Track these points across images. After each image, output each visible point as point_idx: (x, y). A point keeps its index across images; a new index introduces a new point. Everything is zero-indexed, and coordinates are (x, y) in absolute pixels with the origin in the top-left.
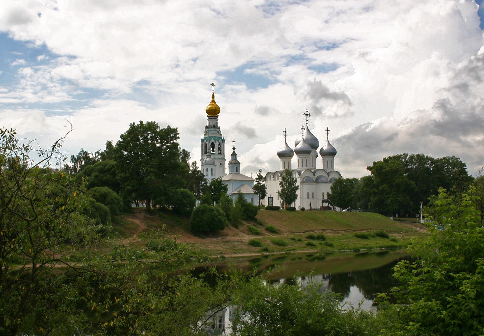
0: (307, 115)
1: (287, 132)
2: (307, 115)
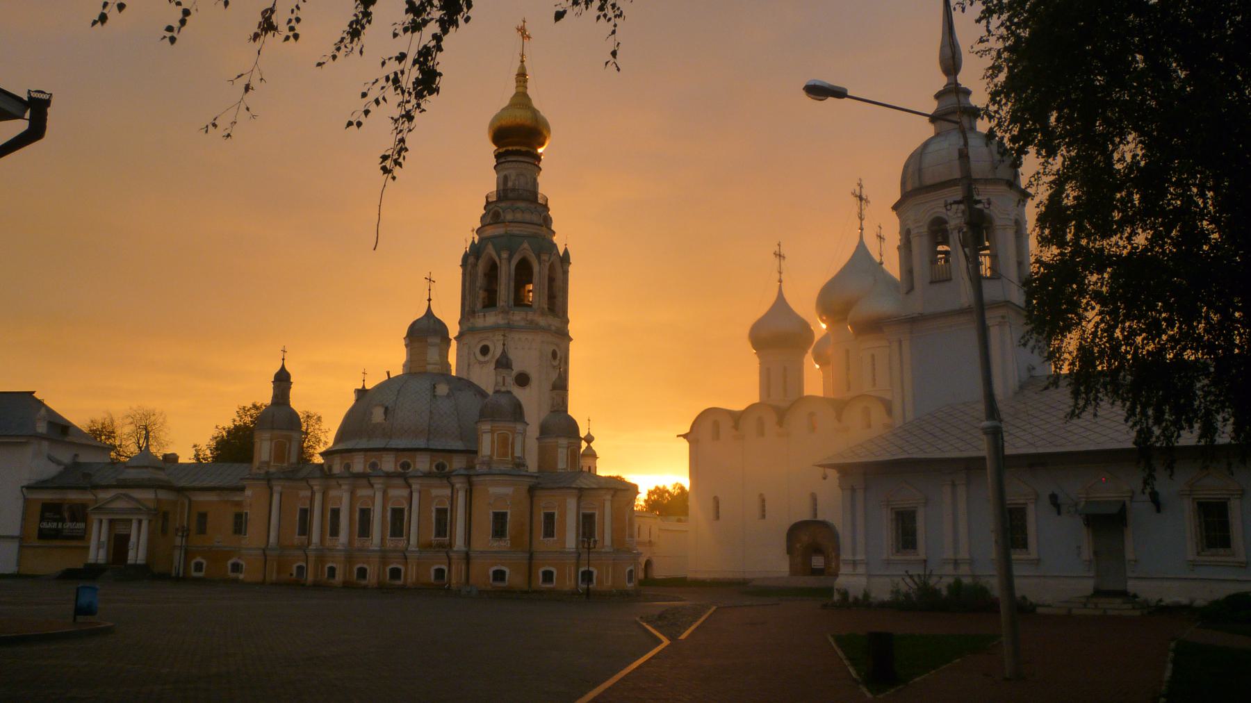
0: (861, 198)
1: (784, 257)
2: (861, 198)
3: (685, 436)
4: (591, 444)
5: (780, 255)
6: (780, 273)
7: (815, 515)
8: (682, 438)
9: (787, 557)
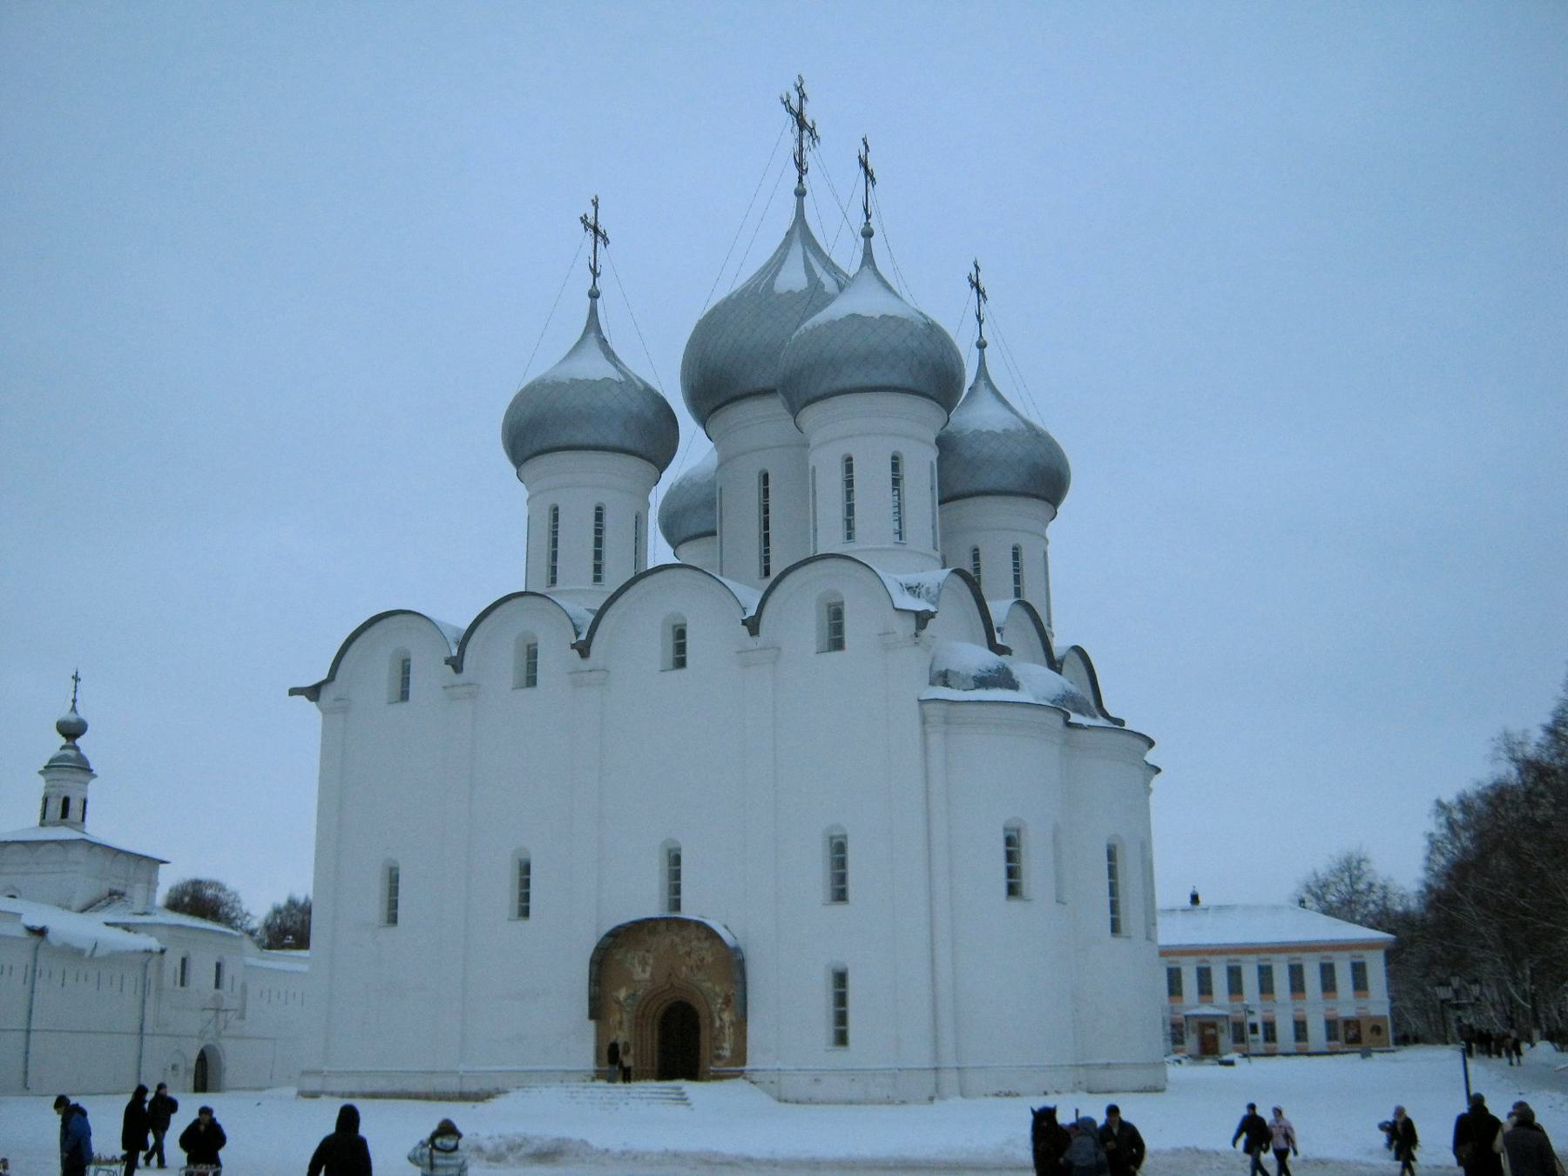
0: (802, 124)
1: (606, 241)
2: (802, 124)
3: (313, 692)
4: (79, 741)
5: (596, 231)
6: (595, 274)
7: (676, 905)
8: (303, 698)
9: (591, 1025)
